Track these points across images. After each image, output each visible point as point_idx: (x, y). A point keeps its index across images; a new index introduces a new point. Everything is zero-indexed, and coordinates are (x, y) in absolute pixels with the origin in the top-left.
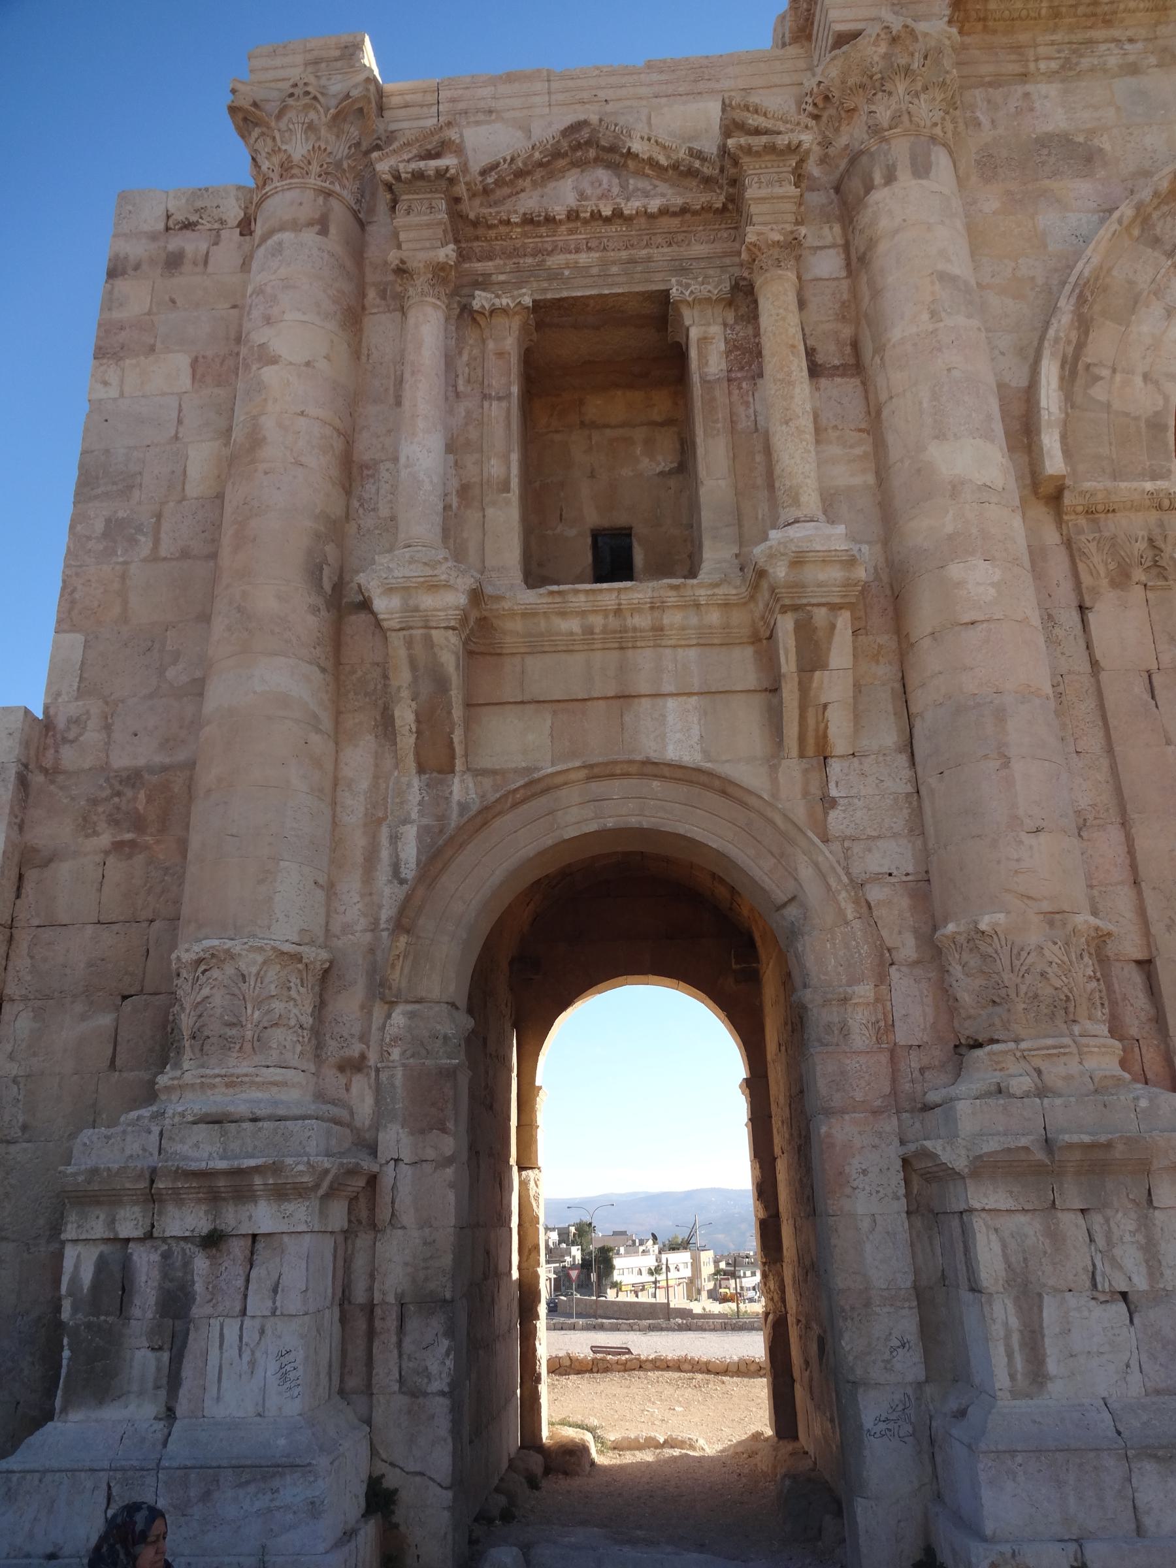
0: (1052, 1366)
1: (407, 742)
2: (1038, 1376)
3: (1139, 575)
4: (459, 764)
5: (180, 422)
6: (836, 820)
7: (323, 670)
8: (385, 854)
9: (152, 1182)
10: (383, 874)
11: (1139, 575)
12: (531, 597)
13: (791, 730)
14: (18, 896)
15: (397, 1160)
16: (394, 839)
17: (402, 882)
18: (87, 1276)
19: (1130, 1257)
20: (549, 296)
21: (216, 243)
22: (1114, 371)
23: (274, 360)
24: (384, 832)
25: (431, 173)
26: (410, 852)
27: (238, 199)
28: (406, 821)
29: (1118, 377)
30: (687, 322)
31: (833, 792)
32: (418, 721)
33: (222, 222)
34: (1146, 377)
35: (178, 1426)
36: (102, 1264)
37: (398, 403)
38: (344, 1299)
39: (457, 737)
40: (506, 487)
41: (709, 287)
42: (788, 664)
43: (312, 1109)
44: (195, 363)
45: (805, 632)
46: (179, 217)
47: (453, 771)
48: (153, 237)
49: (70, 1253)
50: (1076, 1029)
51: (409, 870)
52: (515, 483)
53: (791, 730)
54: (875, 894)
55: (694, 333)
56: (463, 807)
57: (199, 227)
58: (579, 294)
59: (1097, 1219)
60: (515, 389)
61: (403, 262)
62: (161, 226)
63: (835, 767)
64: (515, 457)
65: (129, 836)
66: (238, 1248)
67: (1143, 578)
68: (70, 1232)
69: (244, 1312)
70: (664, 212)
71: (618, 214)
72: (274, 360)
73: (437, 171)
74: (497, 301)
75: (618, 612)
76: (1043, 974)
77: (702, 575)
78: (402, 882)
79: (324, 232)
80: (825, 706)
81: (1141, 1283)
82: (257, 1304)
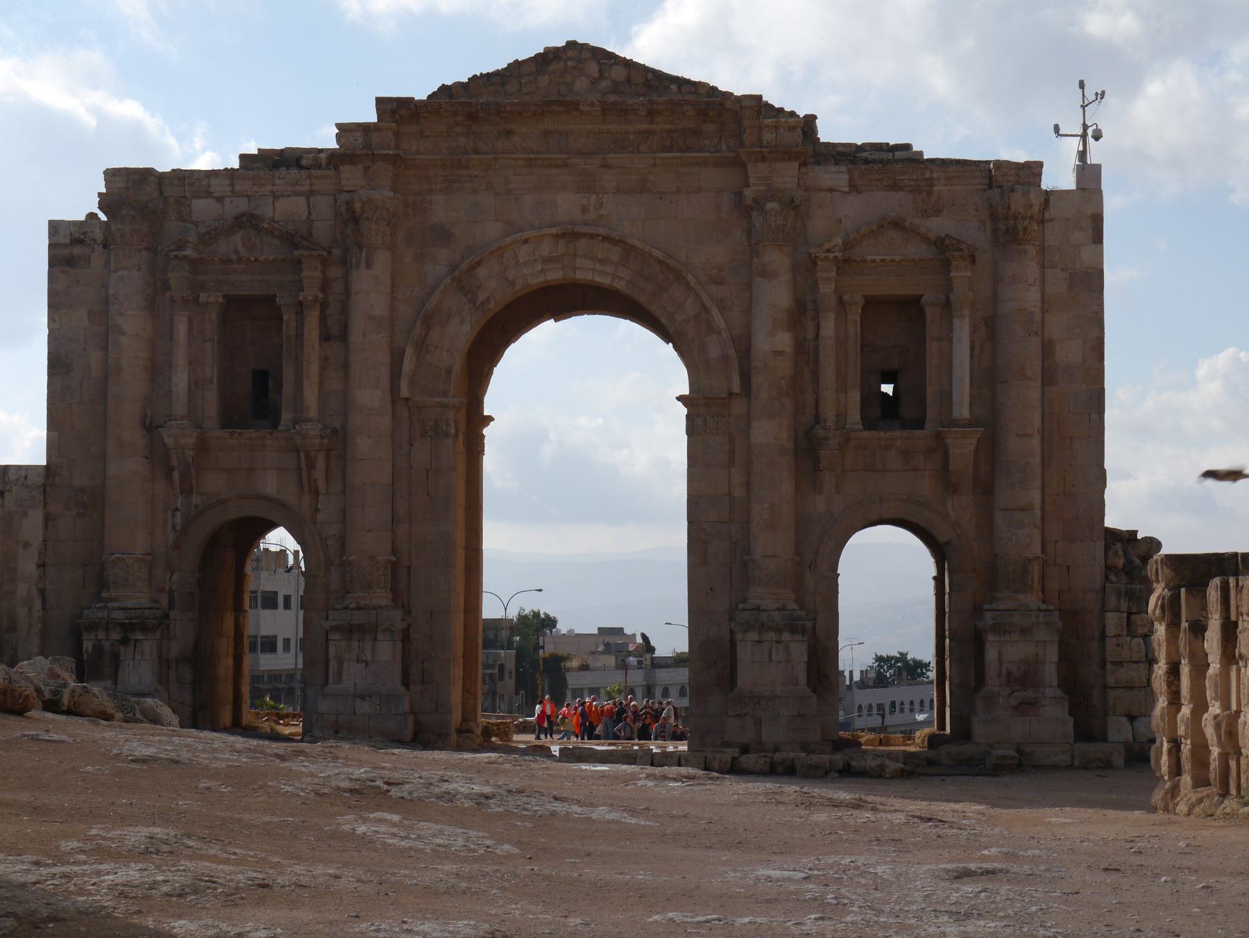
0: (344, 677)
1: (177, 483)
2: (339, 680)
3: (430, 433)
4: (195, 491)
5: (86, 342)
6: (320, 517)
7: (147, 458)
8: (170, 521)
9: (107, 625)
10: (169, 527)
11: (430, 433)
12: (219, 432)
13: (306, 486)
14: (46, 530)
15: (175, 619)
16: (173, 516)
17: (176, 531)
18: (90, 648)
19: (368, 653)
20: (231, 293)
21: (92, 252)
22: (436, 348)
23: (124, 334)
24: (170, 513)
25: (182, 256)
26: (178, 520)
27: (101, 228)
28: (177, 509)
29: (438, 350)
30: (283, 312)
31: (319, 507)
32: (180, 477)
33: (94, 240)
34: (448, 351)
35: (119, 686)
36: (94, 646)
37: (171, 339)
38: (160, 657)
39: (194, 483)
40: (212, 382)
41: (290, 299)
42: (304, 466)
43: (149, 605)
44: (90, 312)
45: (308, 457)
46: (76, 236)
47: (192, 493)
48: (66, 245)
49: (85, 644)
50: (371, 591)
51: (178, 528)
52: (215, 380)
53: (306, 486)
54: (330, 542)
55: (285, 317)
56: (196, 506)
57: (85, 242)
58: (241, 293)
59: (361, 643)
60: (216, 338)
61: (172, 296)
62: (69, 241)
63: (321, 498)
64: (215, 369)
65: (82, 511)
66: (132, 643)
67: (432, 435)
68: (84, 637)
69: (134, 659)
70: (275, 260)
71: (257, 260)
72: (124, 334)
73: (184, 255)
74: (209, 299)
75: (250, 439)
76: (364, 575)
77: (280, 428)
78: (176, 531)
79: (139, 270)
80: (316, 480)
81: (370, 658)
82: (138, 657)
